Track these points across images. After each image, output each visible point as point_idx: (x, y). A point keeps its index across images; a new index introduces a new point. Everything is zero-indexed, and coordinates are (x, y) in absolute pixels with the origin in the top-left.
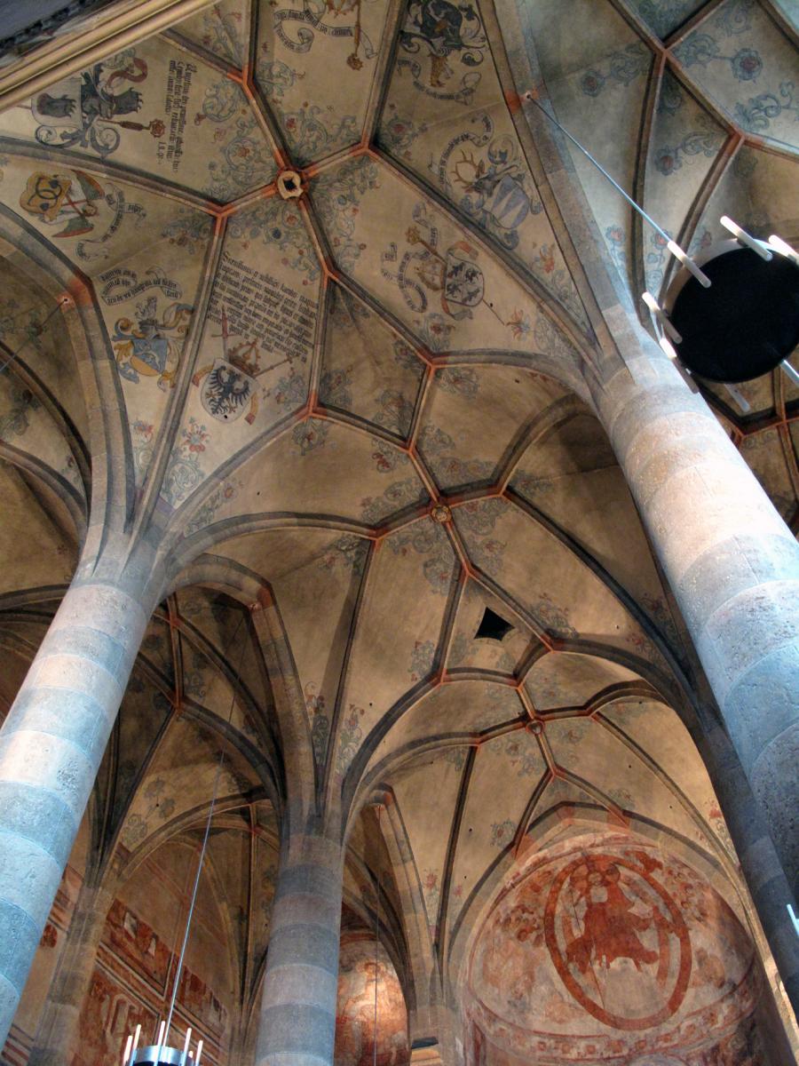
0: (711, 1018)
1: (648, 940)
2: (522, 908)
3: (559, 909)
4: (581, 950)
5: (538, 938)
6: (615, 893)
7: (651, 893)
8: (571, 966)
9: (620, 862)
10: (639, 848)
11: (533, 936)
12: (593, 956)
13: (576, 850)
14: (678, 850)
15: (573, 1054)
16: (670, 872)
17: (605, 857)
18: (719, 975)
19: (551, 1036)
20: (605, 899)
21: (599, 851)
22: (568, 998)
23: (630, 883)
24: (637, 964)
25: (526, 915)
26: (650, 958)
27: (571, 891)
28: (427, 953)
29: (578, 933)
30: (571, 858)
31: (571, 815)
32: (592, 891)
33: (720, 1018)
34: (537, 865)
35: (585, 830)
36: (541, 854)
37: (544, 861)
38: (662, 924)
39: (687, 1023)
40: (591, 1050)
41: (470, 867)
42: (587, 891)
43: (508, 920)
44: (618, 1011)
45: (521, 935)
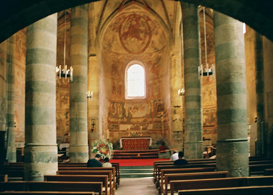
0: (151, 55)
1: (142, 35)
2: (115, 23)
3: (124, 24)
4: (126, 34)
5: (117, 30)
6: (138, 23)
7: (146, 25)
8: (123, 38)
9: (141, 17)
10: (148, 15)
11: (116, 30)
12: (128, 36)
13: (132, 12)
14: (158, 20)
15: (119, 57)
16: (153, 22)
17: (138, 15)
18: (156, 47)
19: (115, 53)
20: (135, 24)
21: (138, 13)
22: (121, 45)
23: (142, 22)
24: (138, 40)
25: (116, 25)
26: (141, 39)
27: (127, 21)
28: (95, 34)
29: (126, 31)
30: (130, 14)
31: (135, 4)
32: (133, 22)
33: (153, 56)
34: (122, 14)
35: (136, 8)
36: (124, 11)
37: (124, 13)
38: (146, 33)
39: (145, 55)
40: (123, 57)
41: (108, 12)
42: (131, 21)
43: (111, 26)
44: (131, 50)
45: (113, 29)
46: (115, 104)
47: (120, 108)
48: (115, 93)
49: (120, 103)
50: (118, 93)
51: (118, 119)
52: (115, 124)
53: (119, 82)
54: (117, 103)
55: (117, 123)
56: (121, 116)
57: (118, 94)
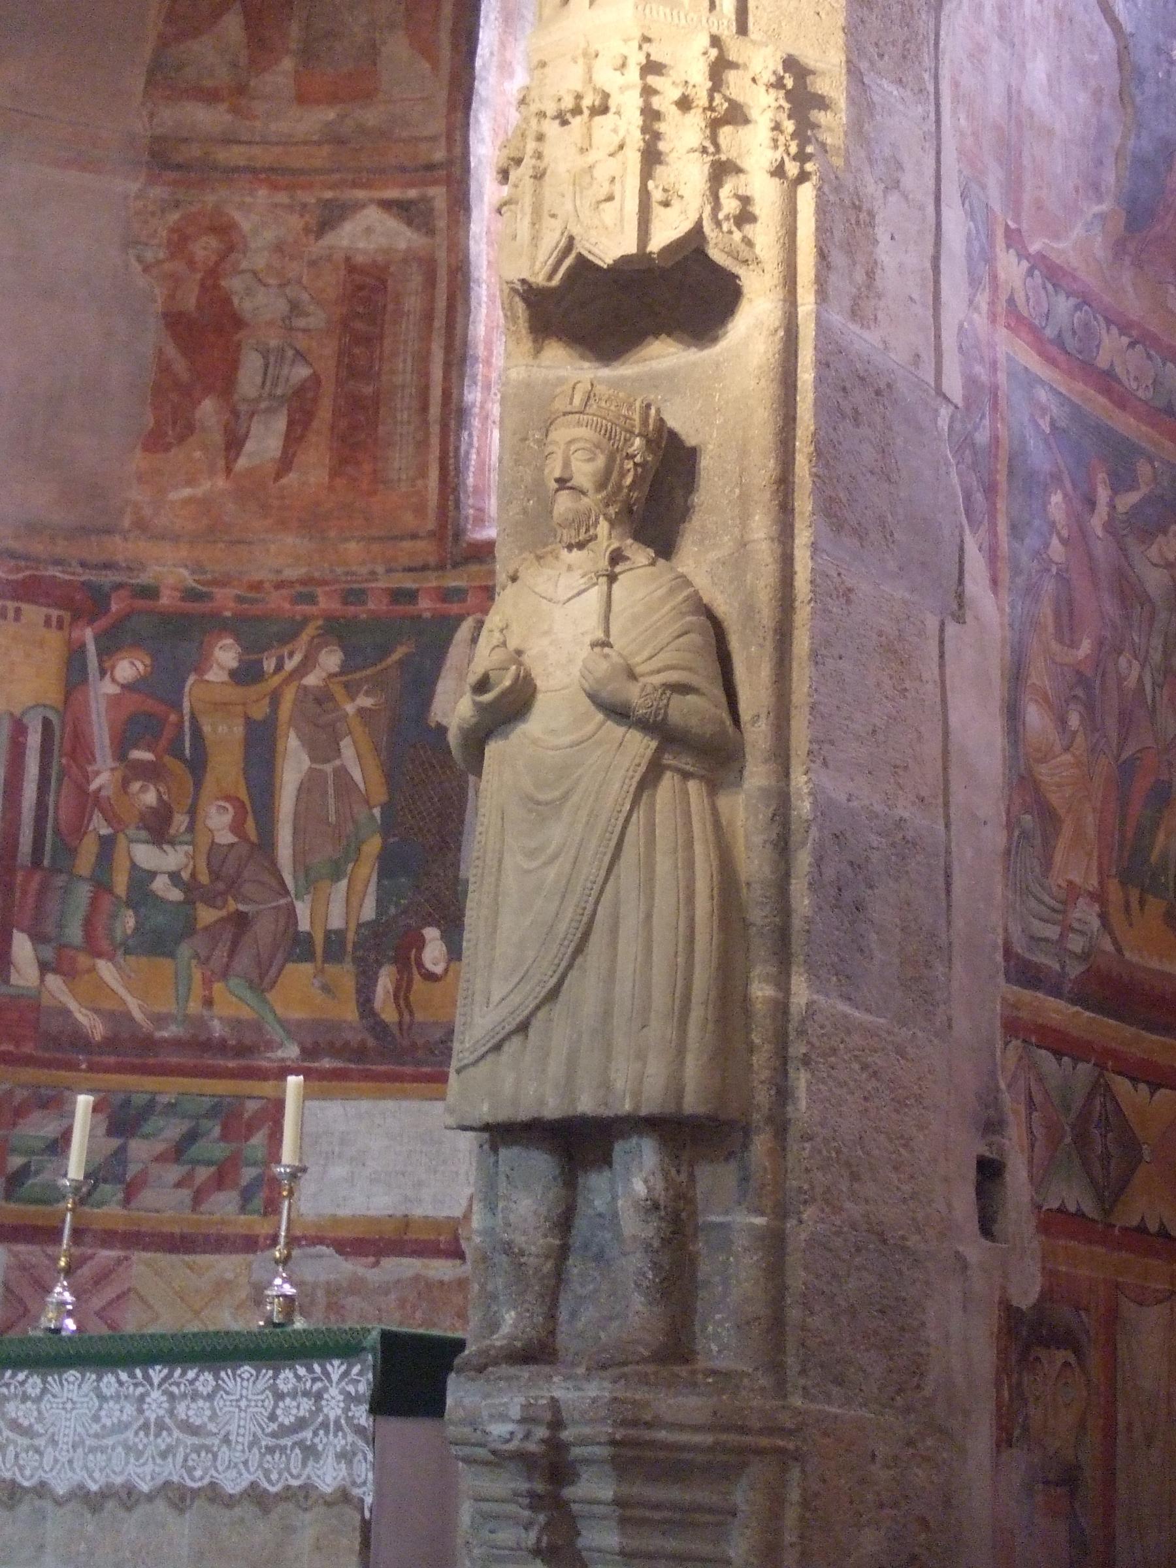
46: (226, 655)
47: (323, 746)
48: (234, 443)
49: (336, 630)
50: (294, 438)
51: (262, 982)
52: (168, 1088)
53: (331, 216)
54: (259, 632)
55: (241, 1054)
56: (344, 905)
57: (285, 463)
